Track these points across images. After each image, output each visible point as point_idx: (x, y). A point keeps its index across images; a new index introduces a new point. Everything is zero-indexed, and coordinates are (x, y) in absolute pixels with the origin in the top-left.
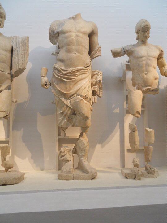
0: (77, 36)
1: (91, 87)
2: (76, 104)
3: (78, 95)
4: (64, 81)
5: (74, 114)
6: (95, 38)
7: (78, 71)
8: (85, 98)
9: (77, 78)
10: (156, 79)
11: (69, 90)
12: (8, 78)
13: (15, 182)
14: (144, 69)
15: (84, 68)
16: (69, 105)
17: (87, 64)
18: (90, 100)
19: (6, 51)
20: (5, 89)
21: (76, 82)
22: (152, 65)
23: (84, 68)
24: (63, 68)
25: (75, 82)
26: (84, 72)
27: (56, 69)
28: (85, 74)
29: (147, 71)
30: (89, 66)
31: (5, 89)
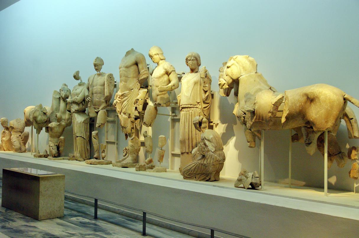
1: (135, 104)
6: (140, 66)
8: (125, 114)
10: (158, 95)
12: (103, 103)
13: (95, 164)
17: (129, 89)
18: (130, 114)
19: (101, 86)
20: (101, 110)
22: (155, 85)
25: (122, 103)
26: (126, 96)
28: (126, 96)
30: (133, 89)
31: (101, 110)
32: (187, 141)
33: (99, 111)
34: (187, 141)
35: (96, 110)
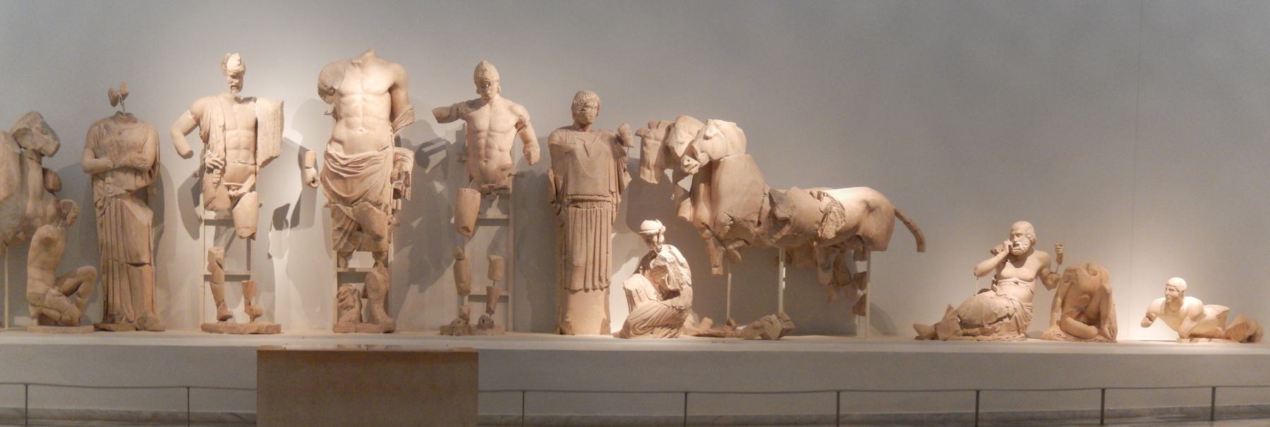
0: (364, 100)
2: (364, 214)
3: (366, 200)
4: (342, 177)
5: (360, 229)
7: (364, 160)
9: (362, 172)
11: (352, 191)
14: (483, 152)
15: (376, 153)
16: (351, 215)
21: (363, 178)
23: (376, 153)
24: (342, 155)
27: (331, 156)
29: (488, 156)
32: (590, 267)
33: (241, 195)
34: (590, 267)
35: (231, 193)
